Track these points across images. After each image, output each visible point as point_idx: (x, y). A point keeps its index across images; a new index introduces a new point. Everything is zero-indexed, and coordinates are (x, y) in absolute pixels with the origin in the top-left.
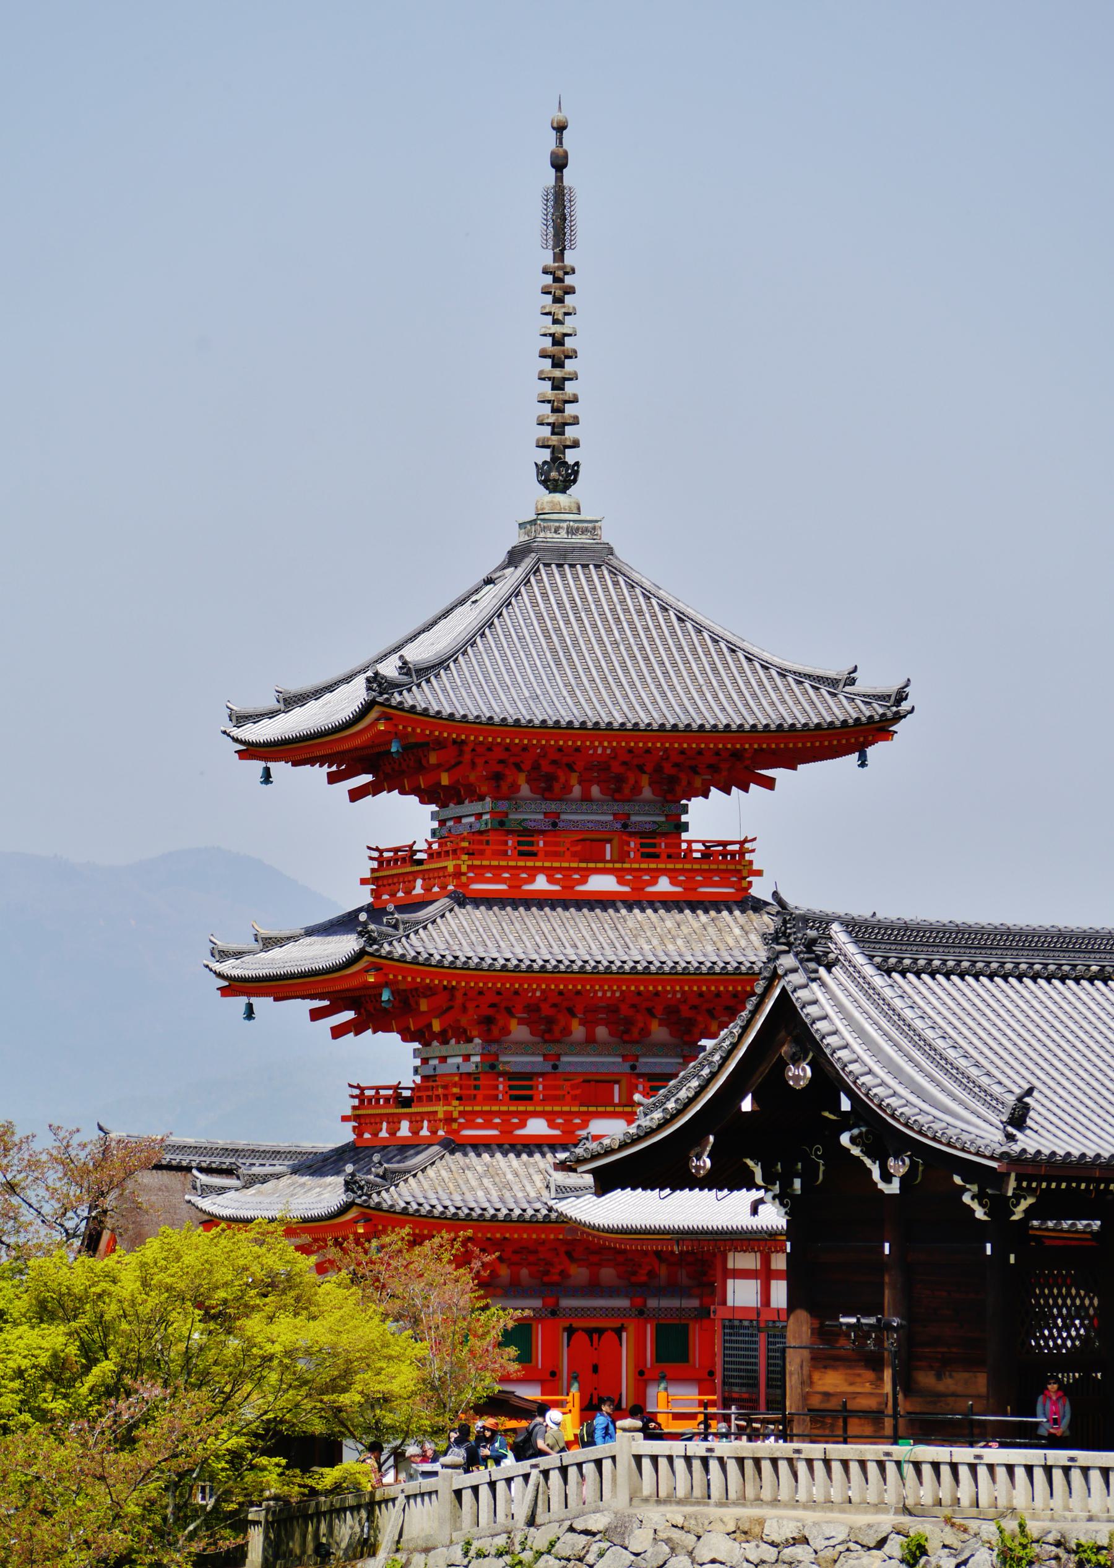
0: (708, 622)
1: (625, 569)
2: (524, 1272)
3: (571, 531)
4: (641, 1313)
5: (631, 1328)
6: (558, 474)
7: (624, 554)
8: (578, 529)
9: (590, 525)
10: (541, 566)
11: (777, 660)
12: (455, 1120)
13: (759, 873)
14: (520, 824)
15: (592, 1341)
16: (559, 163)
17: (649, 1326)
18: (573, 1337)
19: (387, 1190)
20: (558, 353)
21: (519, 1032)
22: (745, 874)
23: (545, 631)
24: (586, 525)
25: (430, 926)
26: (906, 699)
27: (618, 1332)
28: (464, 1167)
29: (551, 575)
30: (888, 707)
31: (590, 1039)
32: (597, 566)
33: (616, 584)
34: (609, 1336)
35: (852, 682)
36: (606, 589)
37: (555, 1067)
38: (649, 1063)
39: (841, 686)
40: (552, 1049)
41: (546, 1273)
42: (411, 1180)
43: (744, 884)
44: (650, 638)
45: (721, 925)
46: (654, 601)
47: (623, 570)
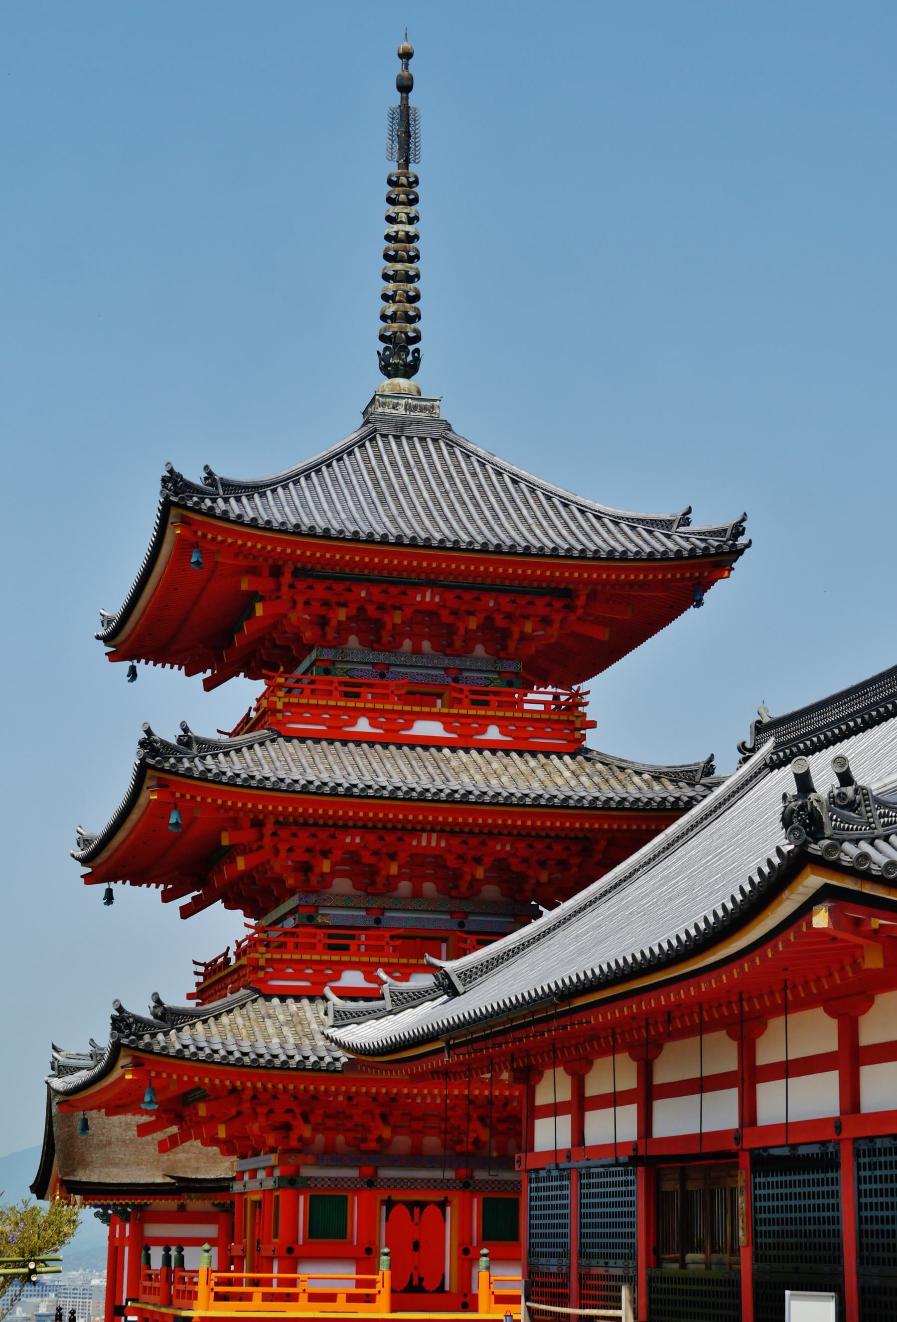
0: (541, 481)
1: (460, 442)
2: (340, 1139)
3: (408, 407)
4: (466, 1185)
5: (456, 1201)
6: (400, 355)
7: (460, 429)
8: (416, 406)
9: (428, 404)
10: (378, 436)
11: (610, 510)
12: (262, 968)
13: (593, 725)
14: (346, 673)
15: (412, 1215)
16: (405, 87)
17: (475, 1201)
18: (392, 1212)
19: (166, 1034)
20: (402, 251)
21: (342, 885)
22: (578, 725)
23: (376, 484)
24: (424, 403)
25: (232, 753)
26: (742, 533)
27: (442, 1205)
28: (265, 1016)
29: (387, 444)
30: (725, 542)
31: (417, 894)
32: (435, 440)
33: (452, 454)
34: (432, 1210)
35: (685, 520)
36: (441, 457)
37: (378, 921)
38: (476, 921)
39: (675, 526)
40: (375, 903)
41: (364, 1140)
42: (199, 1026)
43: (577, 735)
44: (483, 493)
45: (550, 768)
46: (488, 467)
47: (459, 442)
